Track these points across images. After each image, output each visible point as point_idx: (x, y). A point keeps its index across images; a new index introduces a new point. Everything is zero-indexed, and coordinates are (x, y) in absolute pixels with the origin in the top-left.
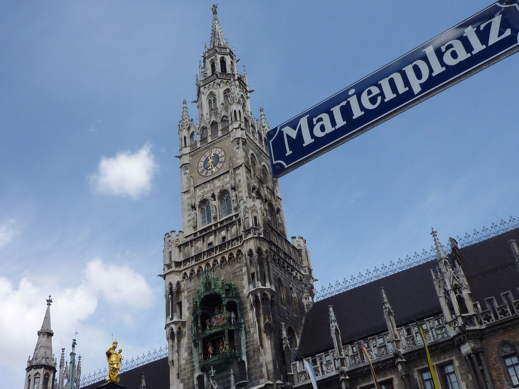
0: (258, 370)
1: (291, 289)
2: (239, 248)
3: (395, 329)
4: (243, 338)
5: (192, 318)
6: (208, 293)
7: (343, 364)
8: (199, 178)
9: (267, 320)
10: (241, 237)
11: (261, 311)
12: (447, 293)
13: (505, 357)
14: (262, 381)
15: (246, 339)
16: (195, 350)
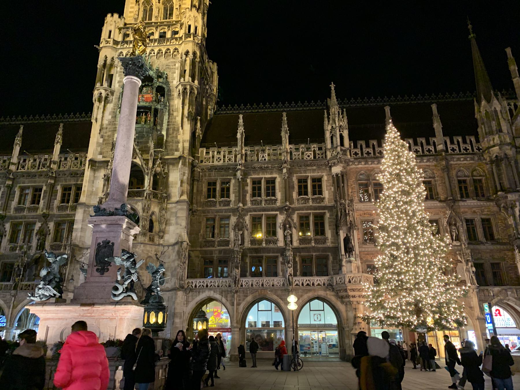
4: (166, 118)
9: (191, 109)
11: (187, 101)
14: (176, 153)
15: (169, 118)
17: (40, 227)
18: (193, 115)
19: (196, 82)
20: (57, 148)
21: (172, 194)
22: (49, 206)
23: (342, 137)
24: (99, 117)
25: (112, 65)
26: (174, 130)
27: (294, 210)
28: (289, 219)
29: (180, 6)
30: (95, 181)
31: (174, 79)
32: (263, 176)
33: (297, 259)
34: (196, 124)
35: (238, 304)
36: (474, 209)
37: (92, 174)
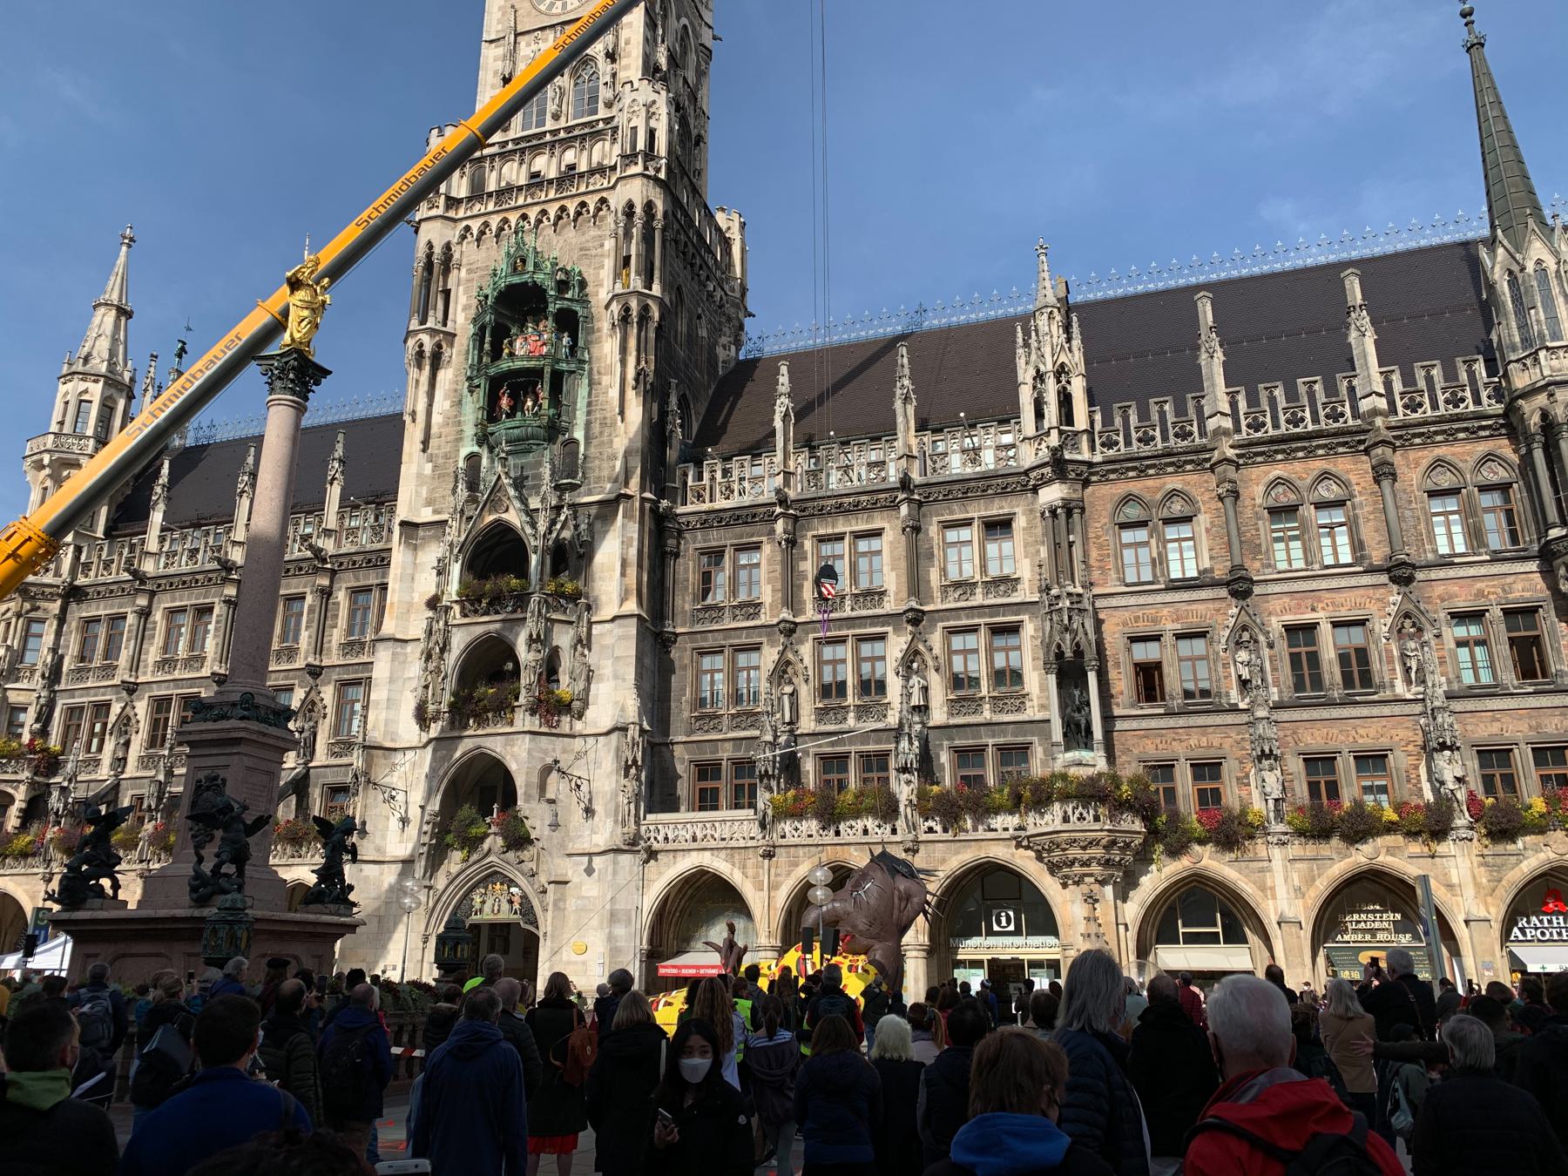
0: (605, 465)
1: (699, 317)
2: (604, 194)
3: (912, 432)
4: (583, 392)
5: (471, 330)
6: (516, 280)
7: (787, 483)
8: (529, 14)
10: (613, 168)
12: (1040, 376)
13: (1124, 526)
16: (469, 398)
17: (303, 702)
18: (650, 379)
19: (656, 289)
20: (334, 493)
21: (603, 598)
22: (319, 647)
23: (1065, 400)
24: (421, 408)
26: (603, 425)
28: (921, 647)
29: (614, 75)
30: (417, 577)
31: (601, 285)
32: (848, 529)
33: (944, 758)
34: (664, 403)
36: (1479, 585)
37: (409, 558)
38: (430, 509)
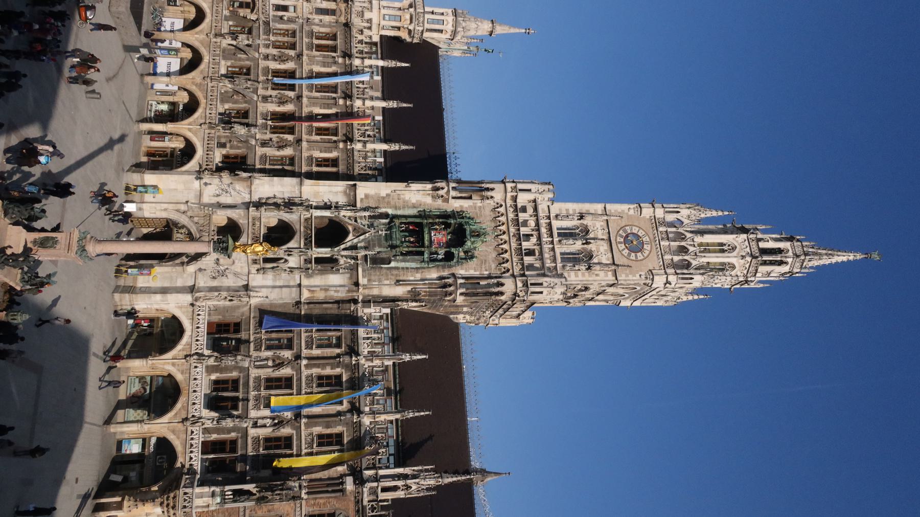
4: (414, 265)
5: (449, 210)
6: (468, 232)
23: (395, 488)
25: (483, 198)
27: (298, 429)
35: (173, 365)
38: (363, 197)
